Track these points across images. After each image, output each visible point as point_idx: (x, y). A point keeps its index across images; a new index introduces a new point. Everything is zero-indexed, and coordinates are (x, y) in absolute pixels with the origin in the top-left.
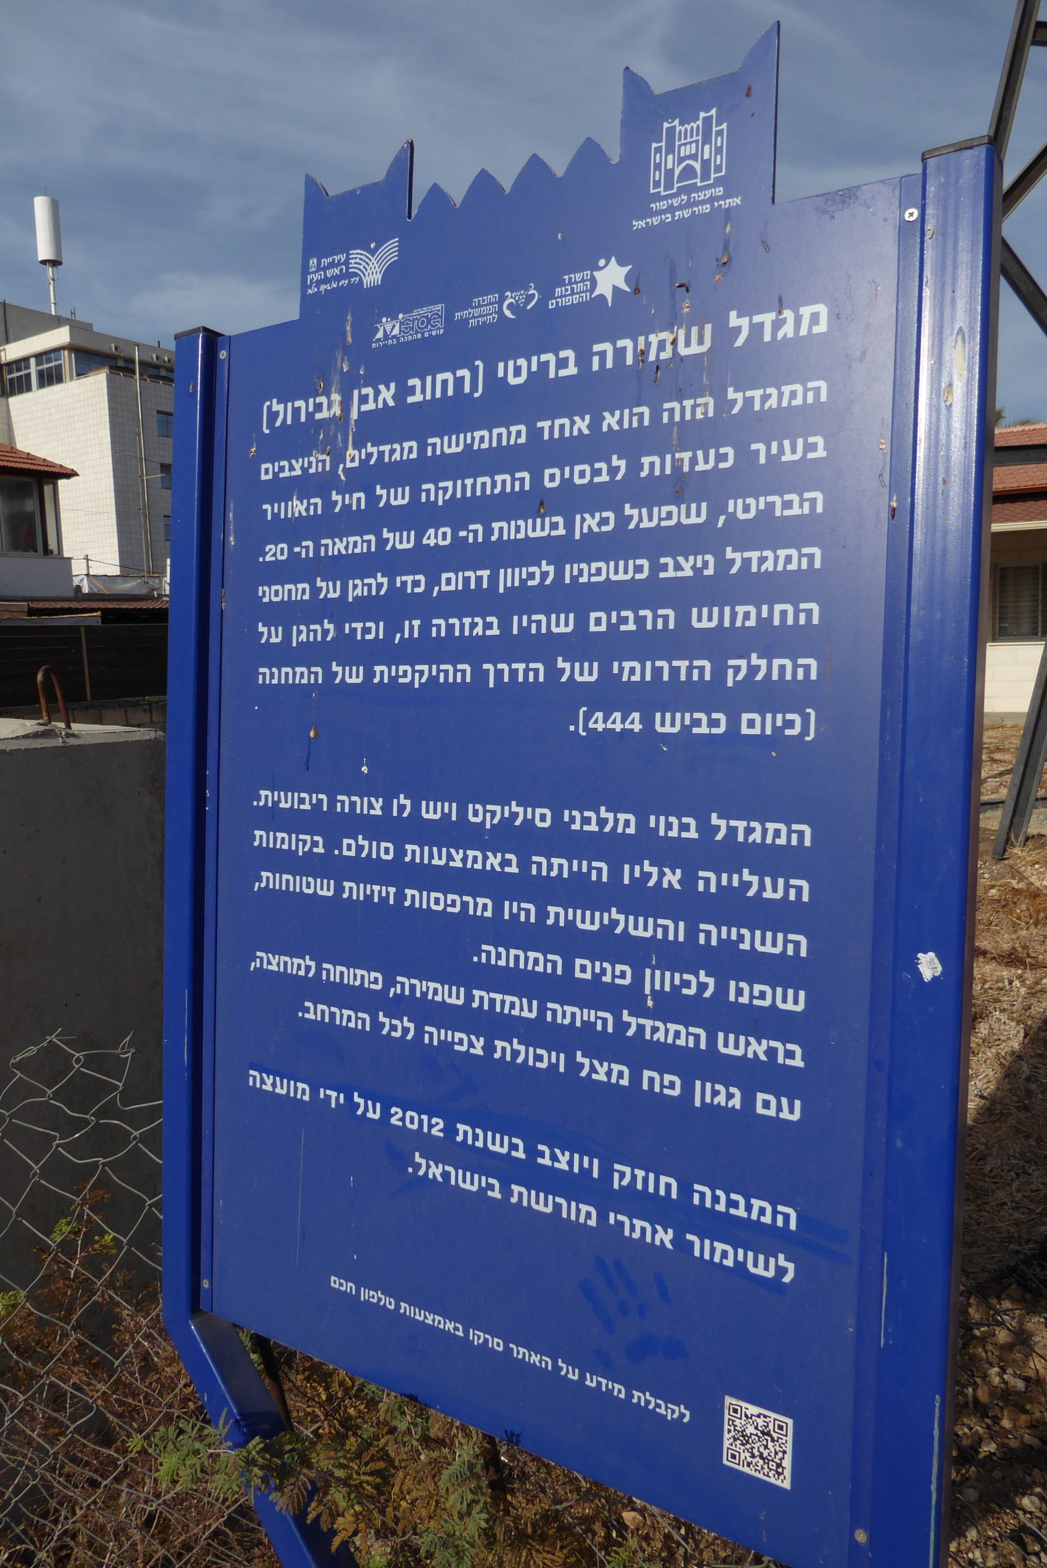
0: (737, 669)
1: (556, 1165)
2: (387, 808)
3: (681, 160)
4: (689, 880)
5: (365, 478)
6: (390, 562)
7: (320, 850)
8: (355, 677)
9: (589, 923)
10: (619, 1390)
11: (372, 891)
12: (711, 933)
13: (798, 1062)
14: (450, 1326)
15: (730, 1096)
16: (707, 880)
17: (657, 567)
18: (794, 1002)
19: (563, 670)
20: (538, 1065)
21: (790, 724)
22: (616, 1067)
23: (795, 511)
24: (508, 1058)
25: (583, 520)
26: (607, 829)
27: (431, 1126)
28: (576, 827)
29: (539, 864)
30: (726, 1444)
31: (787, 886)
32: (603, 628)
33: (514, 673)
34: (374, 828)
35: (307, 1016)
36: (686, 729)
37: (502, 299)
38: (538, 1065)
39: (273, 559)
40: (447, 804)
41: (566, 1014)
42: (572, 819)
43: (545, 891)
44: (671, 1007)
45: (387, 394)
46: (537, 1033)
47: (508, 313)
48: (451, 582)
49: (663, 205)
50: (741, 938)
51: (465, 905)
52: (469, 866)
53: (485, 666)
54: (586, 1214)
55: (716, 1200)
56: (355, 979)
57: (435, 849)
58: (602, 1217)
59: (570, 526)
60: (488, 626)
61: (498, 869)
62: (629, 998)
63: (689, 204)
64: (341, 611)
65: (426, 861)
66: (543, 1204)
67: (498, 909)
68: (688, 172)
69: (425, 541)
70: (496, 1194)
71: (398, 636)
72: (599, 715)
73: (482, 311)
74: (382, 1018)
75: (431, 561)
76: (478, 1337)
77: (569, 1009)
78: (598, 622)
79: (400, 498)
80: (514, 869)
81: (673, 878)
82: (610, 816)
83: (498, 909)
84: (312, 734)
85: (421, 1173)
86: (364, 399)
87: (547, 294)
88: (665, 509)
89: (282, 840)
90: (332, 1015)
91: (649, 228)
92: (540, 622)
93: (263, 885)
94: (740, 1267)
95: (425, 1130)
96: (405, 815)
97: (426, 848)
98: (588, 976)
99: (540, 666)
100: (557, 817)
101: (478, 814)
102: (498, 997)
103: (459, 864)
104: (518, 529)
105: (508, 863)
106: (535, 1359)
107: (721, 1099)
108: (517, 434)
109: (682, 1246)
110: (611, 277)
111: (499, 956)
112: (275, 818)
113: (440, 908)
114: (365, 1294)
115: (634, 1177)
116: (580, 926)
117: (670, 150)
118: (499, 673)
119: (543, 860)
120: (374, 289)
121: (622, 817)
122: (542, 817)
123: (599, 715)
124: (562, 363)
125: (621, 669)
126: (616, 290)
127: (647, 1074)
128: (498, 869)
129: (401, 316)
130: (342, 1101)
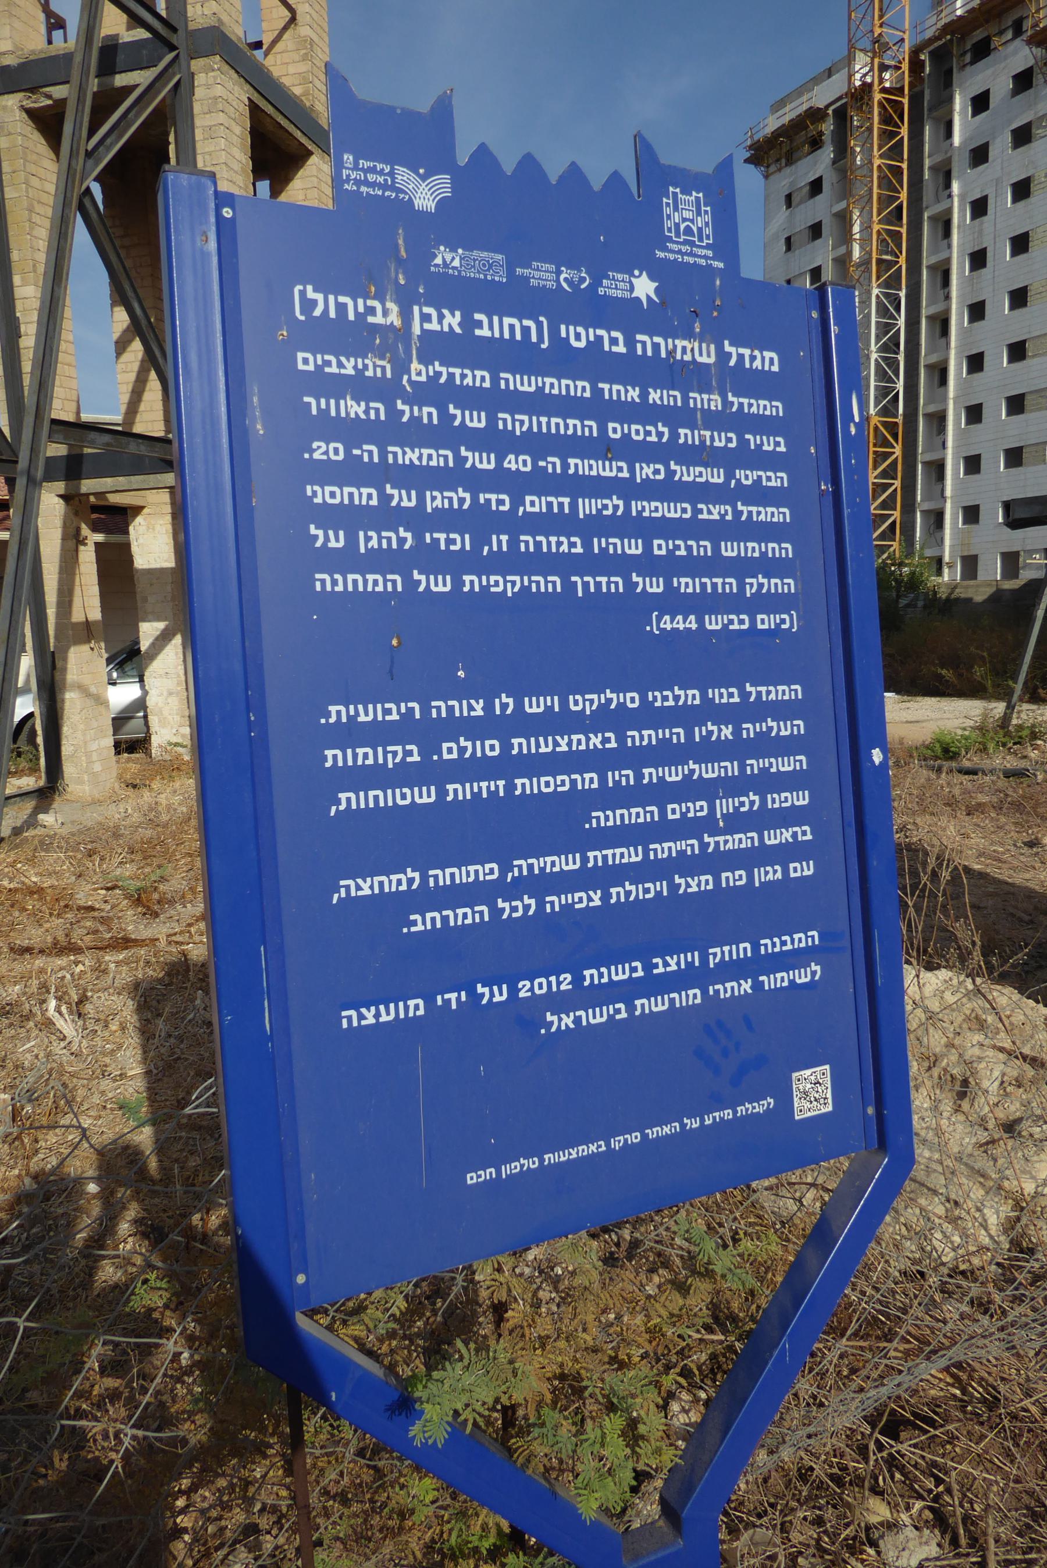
0: (751, 585)
1: (668, 969)
2: (489, 707)
3: (685, 220)
4: (737, 732)
5: (431, 392)
6: (476, 481)
7: (416, 758)
8: (442, 586)
9: (674, 775)
10: (728, 1114)
11: (480, 788)
12: (754, 765)
13: (809, 837)
14: (593, 1148)
15: (775, 872)
16: (748, 729)
17: (696, 511)
18: (802, 799)
19: (637, 583)
20: (647, 896)
21: (783, 621)
22: (703, 878)
23: (773, 484)
24: (623, 900)
25: (642, 468)
26: (681, 703)
27: (559, 983)
28: (658, 704)
29: (633, 737)
30: (796, 1105)
31: (792, 726)
32: (663, 552)
33: (598, 585)
34: (475, 729)
35: (413, 929)
36: (725, 627)
37: (559, 273)
38: (647, 896)
39: (325, 457)
40: (549, 698)
41: (664, 850)
42: (655, 698)
44: (736, 823)
45: (453, 321)
47: (565, 285)
48: (534, 504)
49: (675, 247)
50: (771, 764)
51: (573, 782)
52: (574, 748)
53: (573, 579)
54: (693, 996)
55: (774, 945)
56: (468, 875)
57: (541, 739)
58: (705, 993)
59: (632, 470)
60: (572, 545)
61: (600, 747)
62: (709, 825)
63: (691, 254)
64: (418, 520)
65: (533, 751)
66: (659, 1005)
67: (603, 780)
68: (688, 231)
69: (506, 465)
70: (624, 1015)
71: (486, 549)
72: (667, 618)
73: (541, 274)
74: (501, 904)
75: (518, 485)
76: (618, 1142)
77: (666, 845)
78: (660, 547)
79: (477, 421)
80: (613, 745)
81: (727, 732)
82: (682, 693)
83: (603, 780)
84: (395, 642)
85: (553, 1029)
86: (426, 318)
87: (597, 283)
88: (698, 469)
89: (365, 755)
90: (445, 919)
91: (666, 260)
92: (616, 545)
93: (342, 807)
94: (792, 982)
95: (554, 989)
96: (509, 712)
97: (533, 740)
98: (678, 816)
99: (618, 579)
100: (643, 698)
101: (577, 703)
102: (609, 852)
103: (565, 748)
104: (591, 467)
105: (608, 740)
106: (666, 1130)
107: (770, 877)
108: (582, 388)
109: (757, 986)
110: (644, 287)
111: (607, 818)
112: (350, 734)
113: (551, 789)
114: (506, 1170)
115: (723, 953)
116: (668, 779)
117: (676, 209)
118: (586, 585)
119: (635, 733)
120: (423, 214)
121: (690, 692)
122: (632, 700)
123: (667, 618)
124: (614, 341)
125: (679, 583)
126: (648, 297)
127: (724, 875)
128: (600, 747)
129: (460, 251)
130: (463, 998)
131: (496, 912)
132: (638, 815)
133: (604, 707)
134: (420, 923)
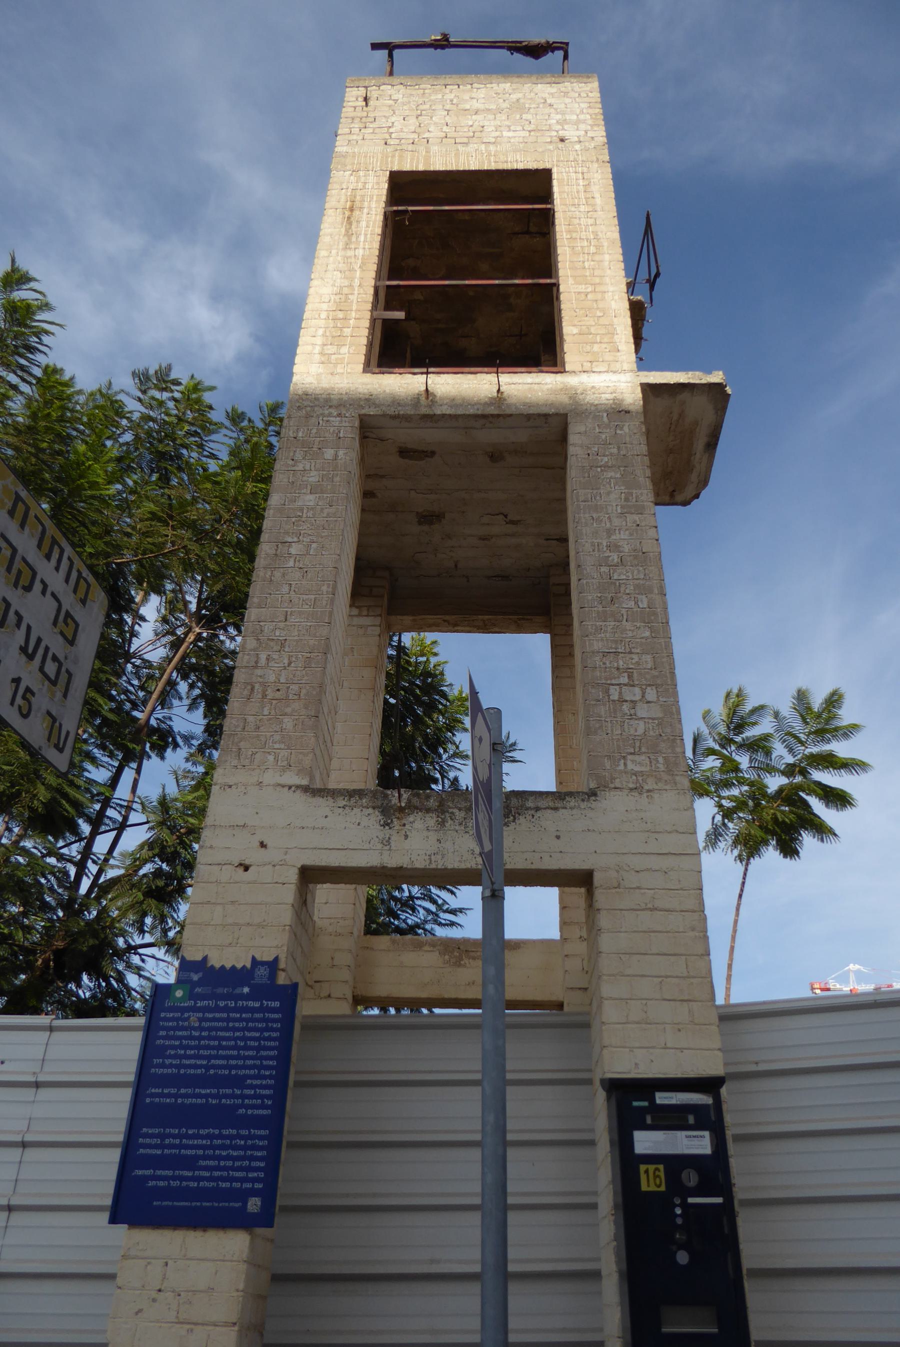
4: (246, 1142)
9: (224, 1153)
18: (262, 1164)
34: (174, 1136)
41: (217, 1174)
43: (214, 1147)
89: (148, 1141)
101: (202, 1132)
122: (217, 1132)
131: (169, 1184)
132: (211, 1163)
134: (151, 1184)
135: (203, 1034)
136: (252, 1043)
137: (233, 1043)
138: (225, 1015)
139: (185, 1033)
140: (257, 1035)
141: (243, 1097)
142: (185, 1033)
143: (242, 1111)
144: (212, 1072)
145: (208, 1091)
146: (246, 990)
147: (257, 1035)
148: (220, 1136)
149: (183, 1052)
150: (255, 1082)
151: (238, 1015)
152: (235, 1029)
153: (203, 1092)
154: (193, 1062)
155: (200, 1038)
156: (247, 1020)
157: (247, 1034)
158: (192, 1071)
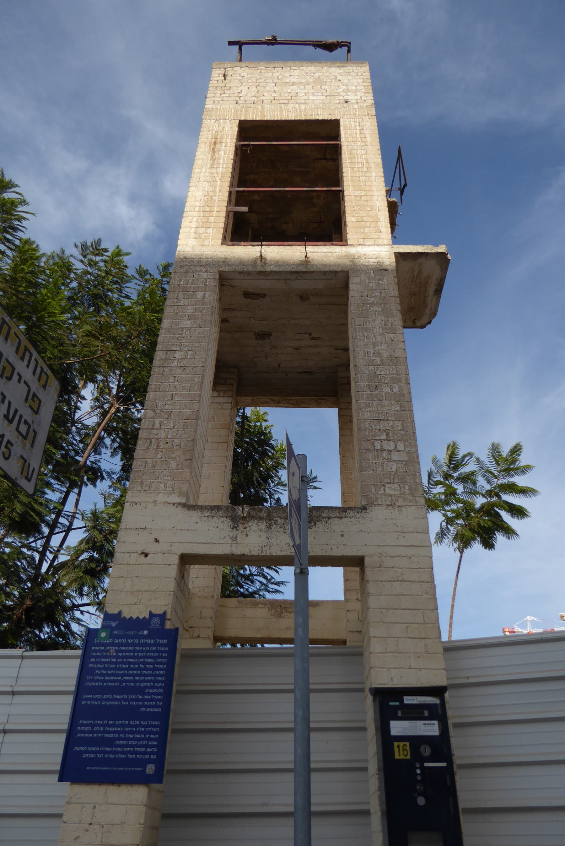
9: (131, 736)
12: (147, 736)
18: (156, 743)
41: (127, 749)
46: (121, 753)
62: (137, 746)
89: (83, 728)
101: (117, 723)
122: (127, 722)
131: (97, 756)
132: (123, 742)
133: (121, 724)
134: (85, 756)
135: (118, 660)
136: (149, 666)
137: (137, 666)
138: (132, 648)
139: (107, 660)
140: (153, 661)
141: (144, 700)
142: (107, 660)
143: (143, 709)
144: (124, 684)
145: (122, 697)
146: (146, 632)
147: (153, 661)
148: (129, 725)
149: (105, 672)
150: (151, 691)
151: (141, 648)
152: (138, 657)
153: (118, 697)
154: (112, 678)
155: (116, 663)
156: (146, 652)
157: (147, 660)
158: (111, 684)
